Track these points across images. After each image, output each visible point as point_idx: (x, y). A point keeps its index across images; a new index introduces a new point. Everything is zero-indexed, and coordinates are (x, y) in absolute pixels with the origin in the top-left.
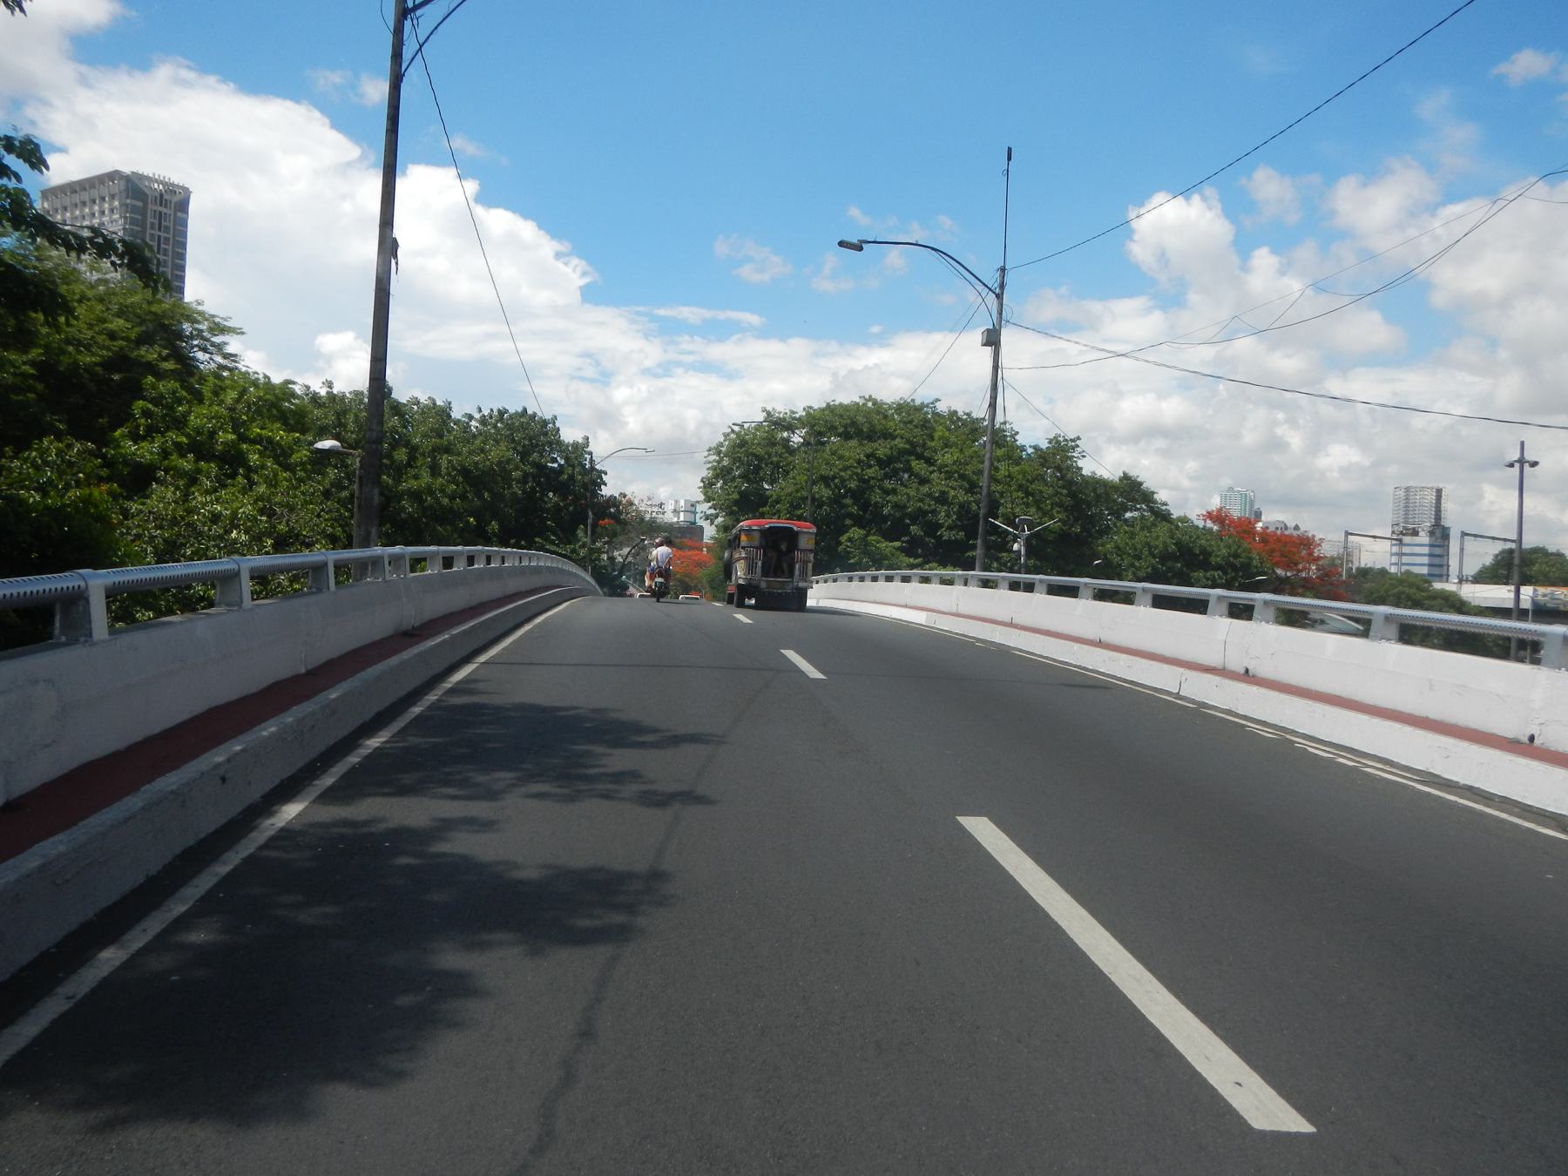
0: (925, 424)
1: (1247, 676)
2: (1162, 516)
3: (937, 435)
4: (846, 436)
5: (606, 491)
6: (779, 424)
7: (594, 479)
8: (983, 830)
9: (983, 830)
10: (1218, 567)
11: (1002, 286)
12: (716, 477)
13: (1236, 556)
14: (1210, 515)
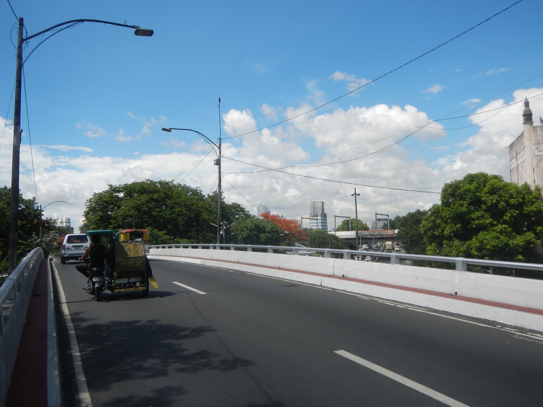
0: (170, 188)
1: (343, 277)
2: (248, 216)
4: (142, 194)
5: (44, 218)
6: (114, 190)
7: (38, 213)
8: (342, 353)
9: (342, 353)
10: (268, 232)
11: (220, 144)
12: (91, 211)
13: (274, 228)
14: (263, 215)
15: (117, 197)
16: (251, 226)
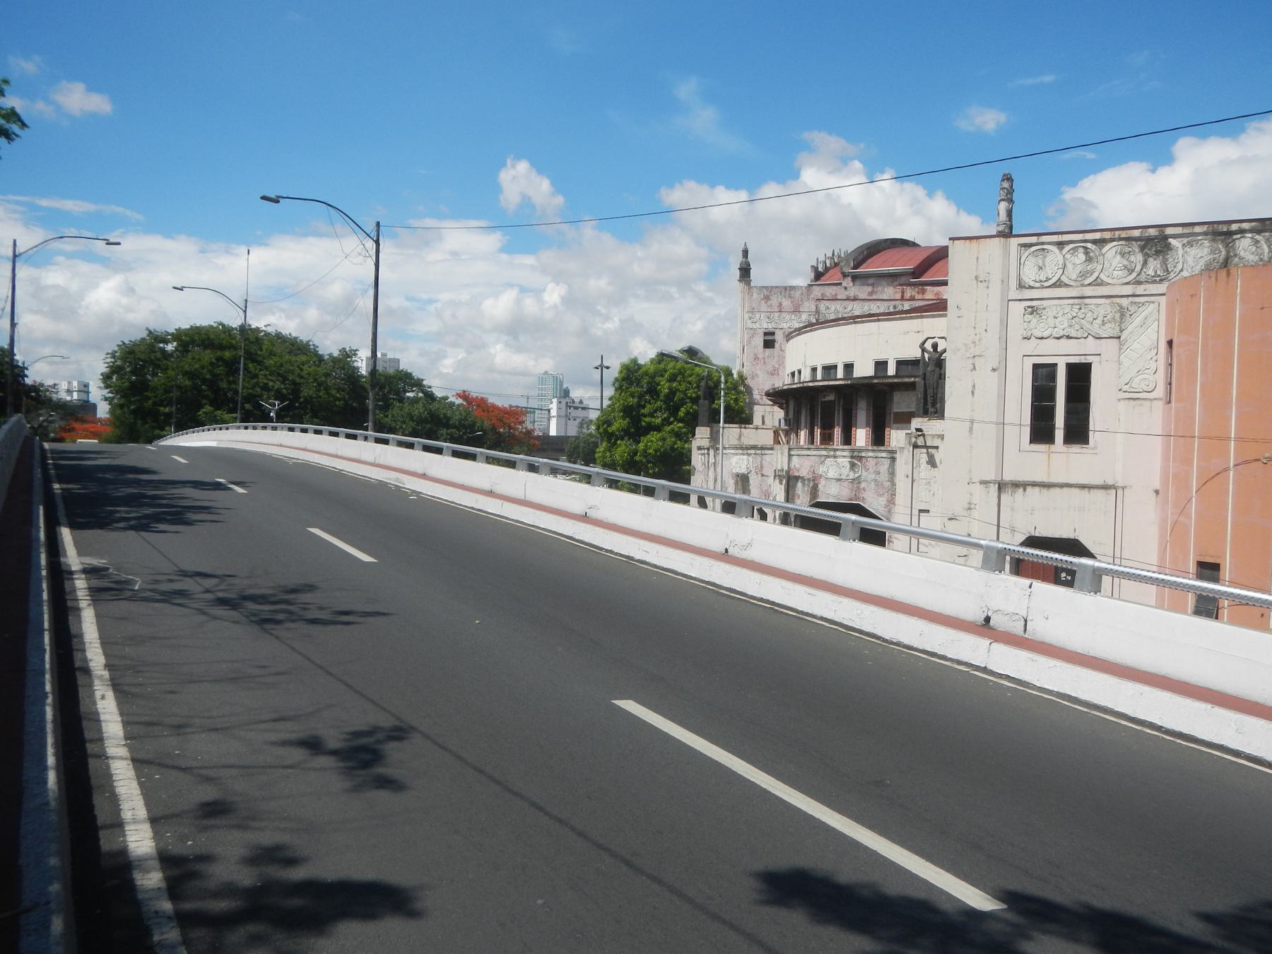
0: (258, 341)
2: (430, 396)
3: (264, 347)
5: (28, 381)
6: (157, 337)
14: (459, 395)
15: (163, 351)
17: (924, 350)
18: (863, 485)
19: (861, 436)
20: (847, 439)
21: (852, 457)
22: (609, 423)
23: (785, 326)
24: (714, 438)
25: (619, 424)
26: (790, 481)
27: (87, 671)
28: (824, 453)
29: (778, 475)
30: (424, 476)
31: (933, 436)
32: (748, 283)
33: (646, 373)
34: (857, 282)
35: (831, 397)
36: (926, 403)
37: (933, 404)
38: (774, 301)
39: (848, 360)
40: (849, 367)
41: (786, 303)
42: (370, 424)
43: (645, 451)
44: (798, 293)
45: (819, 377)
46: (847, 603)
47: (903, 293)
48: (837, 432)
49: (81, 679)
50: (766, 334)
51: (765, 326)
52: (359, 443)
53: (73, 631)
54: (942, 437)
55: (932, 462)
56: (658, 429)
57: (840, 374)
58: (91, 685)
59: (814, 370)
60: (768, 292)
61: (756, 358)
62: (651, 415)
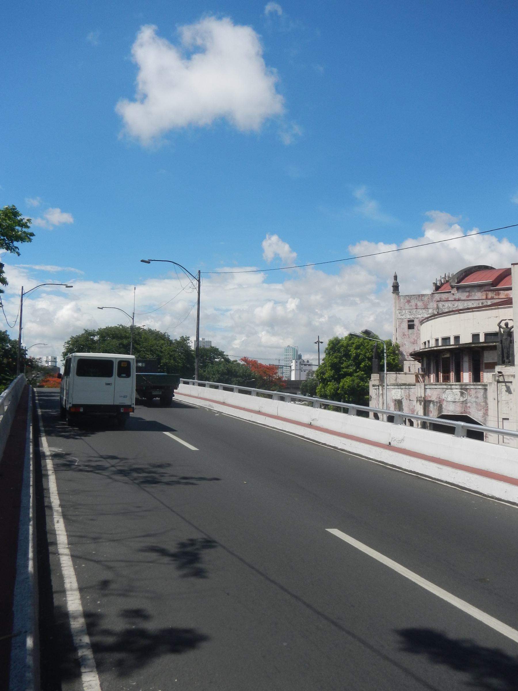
0: (139, 334)
2: (227, 361)
3: (143, 337)
4: (113, 338)
5: (27, 357)
7: (23, 352)
10: (240, 376)
15: (92, 339)
16: (222, 370)
17: (500, 327)
18: (469, 405)
19: (466, 377)
20: (458, 379)
21: (461, 389)
22: (323, 373)
23: (419, 316)
24: (382, 380)
25: (329, 373)
26: (426, 403)
27: (50, 508)
28: (445, 387)
29: (419, 400)
30: (224, 404)
31: (508, 376)
32: (398, 294)
33: (342, 346)
34: (460, 291)
35: (448, 355)
36: (503, 357)
37: (507, 357)
38: (413, 303)
39: (457, 334)
40: (457, 338)
41: (420, 304)
42: (195, 376)
43: (343, 387)
44: (426, 299)
45: (440, 344)
46: (460, 473)
47: (487, 295)
48: (452, 375)
49: (47, 512)
50: (409, 321)
51: (408, 317)
52: (190, 386)
53: (45, 487)
54: (514, 376)
55: (509, 391)
56: (351, 374)
57: (452, 342)
58: (52, 515)
59: (437, 340)
60: (409, 298)
61: (404, 335)
62: (347, 367)
